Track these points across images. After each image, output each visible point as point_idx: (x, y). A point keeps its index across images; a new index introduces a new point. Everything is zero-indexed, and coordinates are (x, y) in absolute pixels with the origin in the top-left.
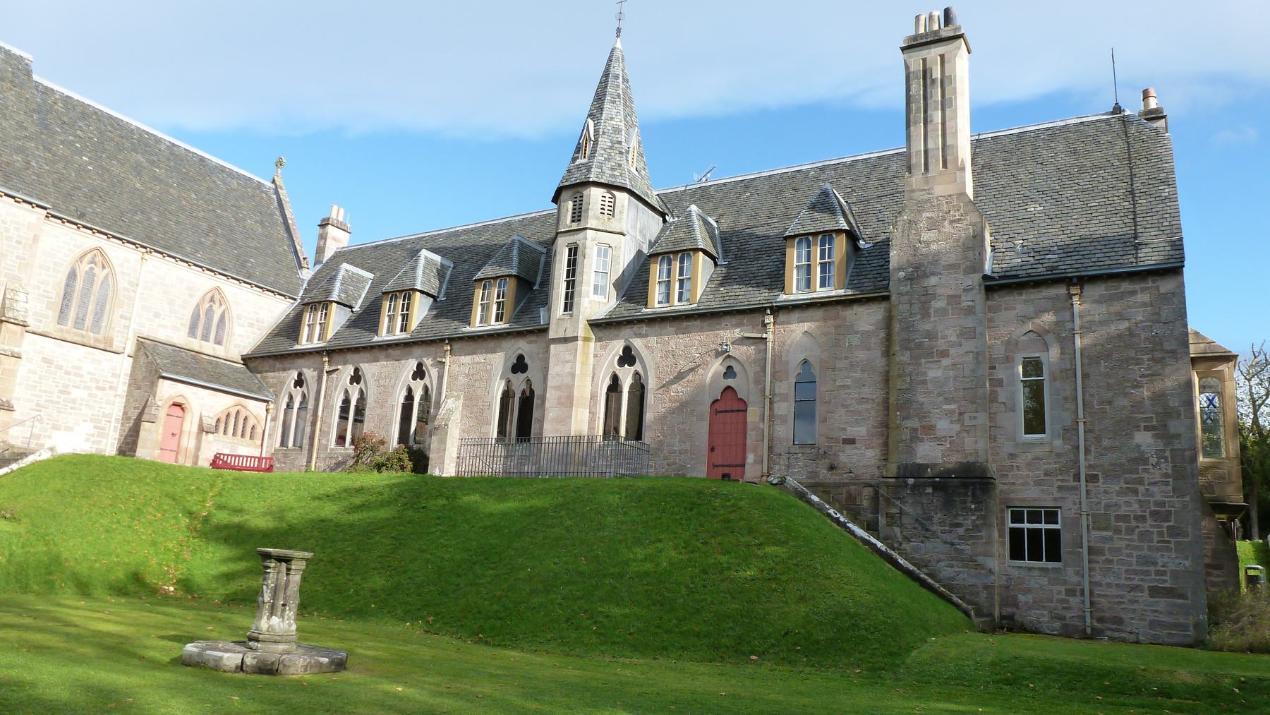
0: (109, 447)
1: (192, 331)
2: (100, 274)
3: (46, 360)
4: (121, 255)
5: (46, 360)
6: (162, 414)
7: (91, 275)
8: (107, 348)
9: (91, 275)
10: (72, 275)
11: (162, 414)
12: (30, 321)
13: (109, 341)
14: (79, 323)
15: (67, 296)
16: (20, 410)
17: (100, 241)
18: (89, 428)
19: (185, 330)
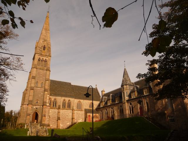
0: (84, 121)
1: (90, 107)
2: (80, 103)
3: (77, 113)
4: (82, 101)
5: (77, 113)
6: (88, 117)
7: (79, 103)
8: (82, 111)
9: (79, 103)
10: (78, 104)
11: (88, 117)
12: (75, 109)
13: (82, 110)
14: (79, 109)
15: (78, 106)
16: (75, 118)
17: (80, 100)
18: (81, 119)
19: (89, 107)
